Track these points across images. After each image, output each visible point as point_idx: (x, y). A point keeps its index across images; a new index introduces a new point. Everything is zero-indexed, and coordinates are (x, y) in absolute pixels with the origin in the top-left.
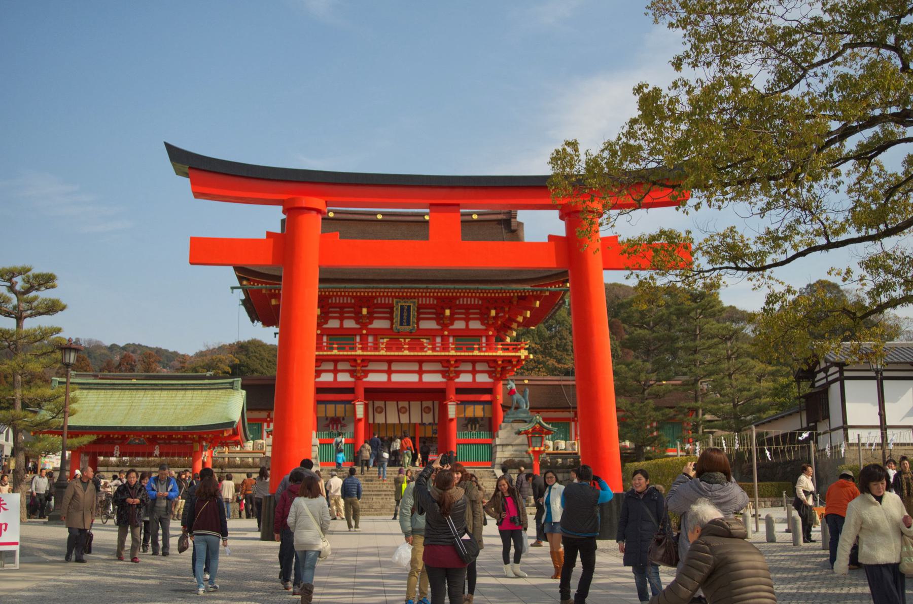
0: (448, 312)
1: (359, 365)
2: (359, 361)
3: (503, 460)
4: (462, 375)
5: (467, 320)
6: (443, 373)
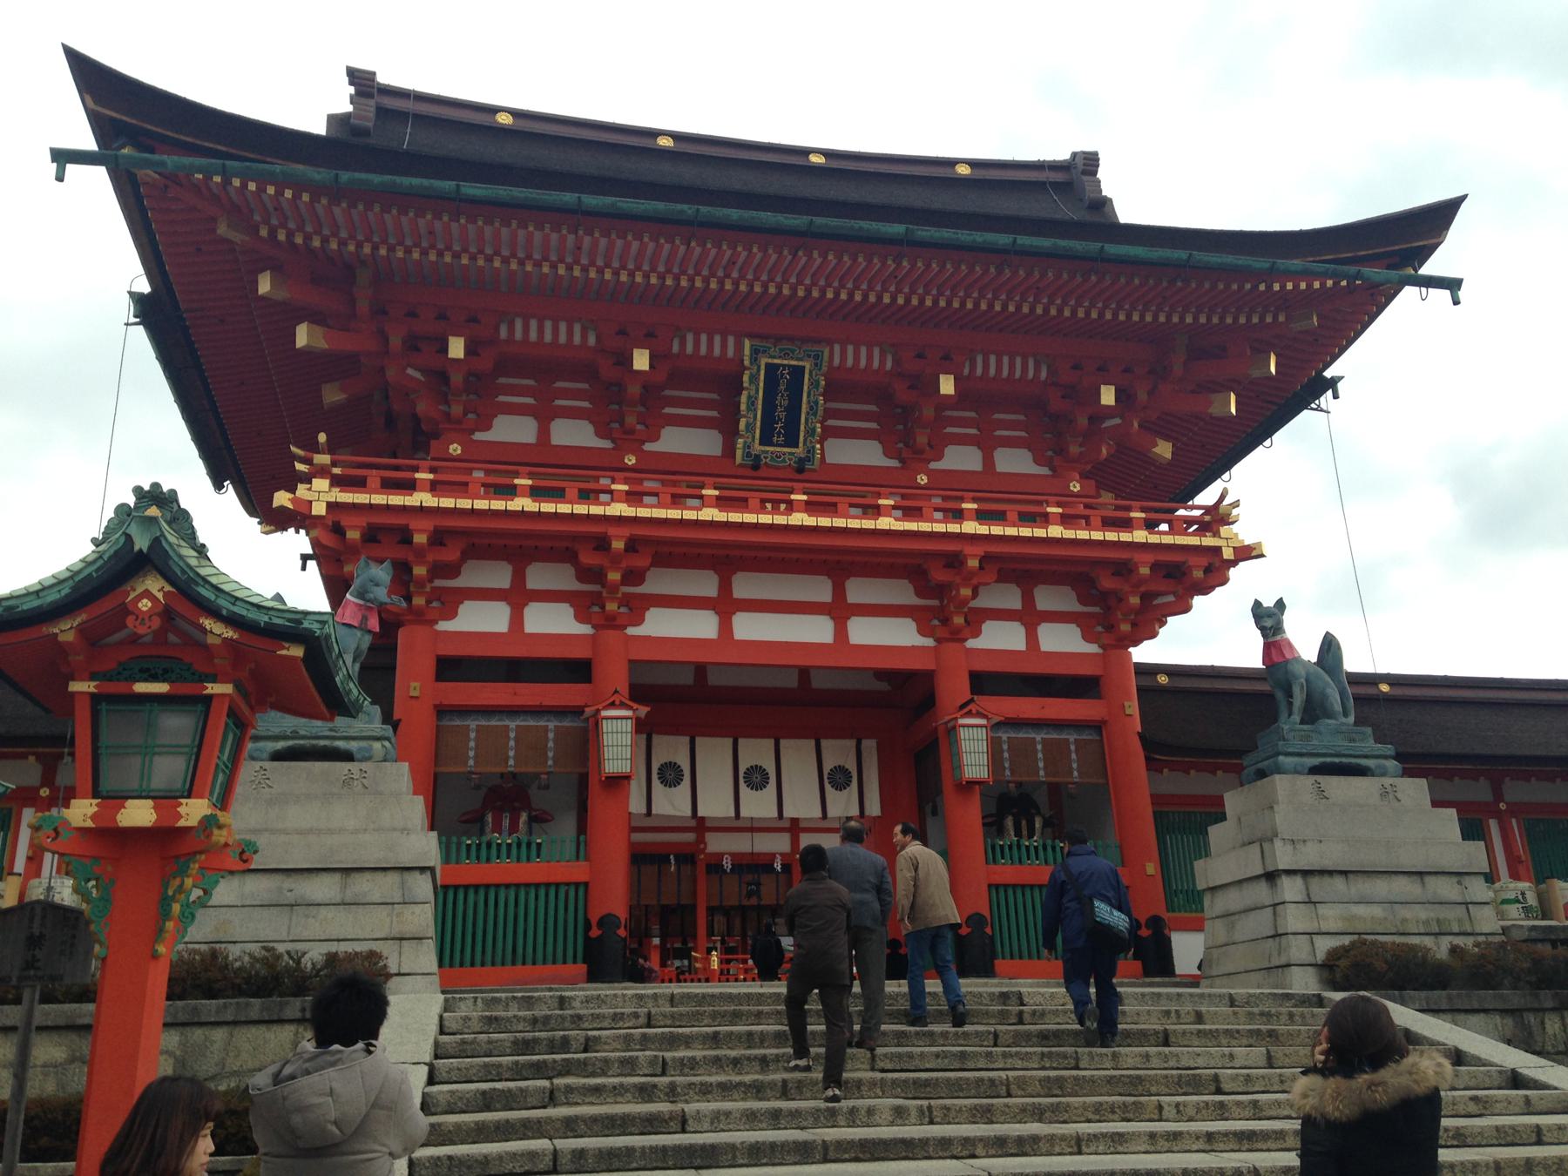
1: (615, 560)
2: (618, 545)
3: (1324, 945)
4: (989, 627)
5: (987, 446)
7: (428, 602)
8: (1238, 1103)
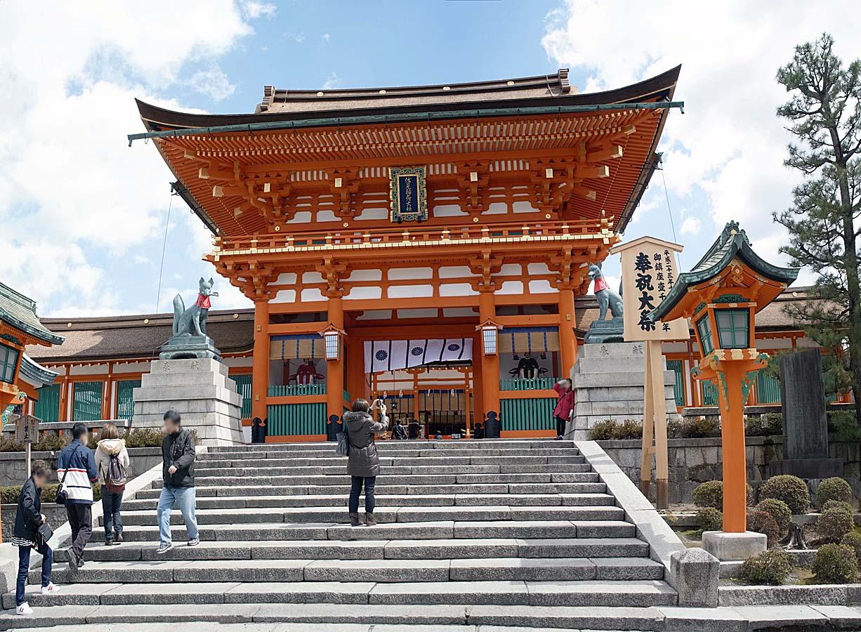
0: (474, 177)
2: (327, 262)
4: (505, 284)
5: (510, 202)
6: (475, 283)
7: (265, 293)
8: (443, 488)
